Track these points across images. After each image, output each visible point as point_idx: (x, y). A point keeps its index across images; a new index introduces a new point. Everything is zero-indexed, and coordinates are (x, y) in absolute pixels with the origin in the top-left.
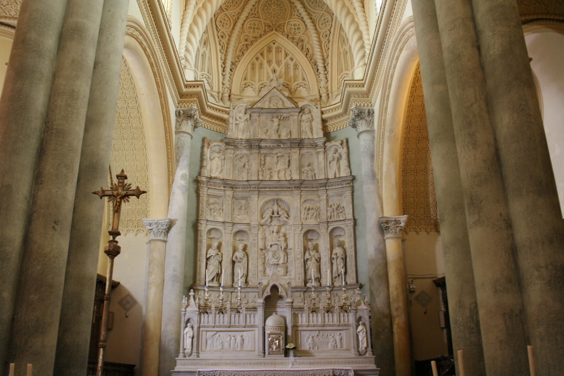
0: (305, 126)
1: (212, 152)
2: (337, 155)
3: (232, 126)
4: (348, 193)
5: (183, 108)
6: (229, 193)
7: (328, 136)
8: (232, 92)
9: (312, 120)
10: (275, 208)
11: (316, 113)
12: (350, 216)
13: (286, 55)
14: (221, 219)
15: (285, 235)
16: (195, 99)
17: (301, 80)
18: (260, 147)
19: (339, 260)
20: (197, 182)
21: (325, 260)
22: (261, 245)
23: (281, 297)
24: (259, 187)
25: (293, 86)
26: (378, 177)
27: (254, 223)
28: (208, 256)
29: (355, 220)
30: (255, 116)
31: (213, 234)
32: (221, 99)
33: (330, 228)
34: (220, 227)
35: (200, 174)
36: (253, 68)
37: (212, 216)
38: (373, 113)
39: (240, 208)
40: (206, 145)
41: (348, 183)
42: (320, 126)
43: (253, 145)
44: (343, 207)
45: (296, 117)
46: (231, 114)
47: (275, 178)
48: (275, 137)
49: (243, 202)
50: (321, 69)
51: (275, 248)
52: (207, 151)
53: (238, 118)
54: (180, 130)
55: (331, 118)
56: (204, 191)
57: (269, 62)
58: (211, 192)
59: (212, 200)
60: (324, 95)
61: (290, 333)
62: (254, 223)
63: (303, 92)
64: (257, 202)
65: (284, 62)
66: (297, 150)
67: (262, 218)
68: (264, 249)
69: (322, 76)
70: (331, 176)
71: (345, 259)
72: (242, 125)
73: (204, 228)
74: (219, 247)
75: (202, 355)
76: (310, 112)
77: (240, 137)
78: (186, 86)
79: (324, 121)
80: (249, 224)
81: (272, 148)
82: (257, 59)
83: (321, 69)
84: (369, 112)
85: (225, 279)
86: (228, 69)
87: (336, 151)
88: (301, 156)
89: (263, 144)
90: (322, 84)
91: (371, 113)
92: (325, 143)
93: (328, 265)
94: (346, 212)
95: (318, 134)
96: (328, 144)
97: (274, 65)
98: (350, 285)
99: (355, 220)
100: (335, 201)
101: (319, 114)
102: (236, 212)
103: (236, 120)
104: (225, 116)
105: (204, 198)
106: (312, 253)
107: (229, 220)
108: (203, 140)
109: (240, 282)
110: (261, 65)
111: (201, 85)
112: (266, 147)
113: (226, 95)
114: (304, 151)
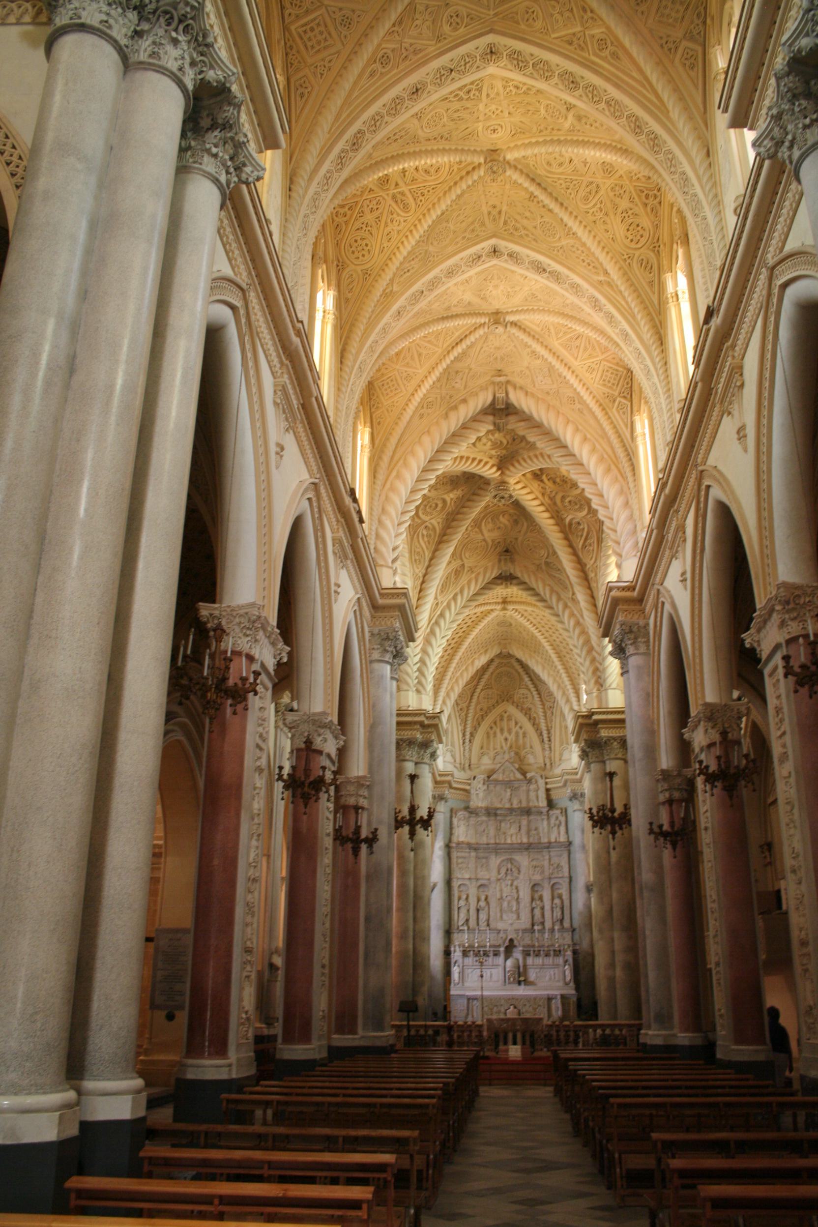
0: (532, 794)
1: (459, 820)
2: (557, 822)
3: (473, 797)
4: (565, 855)
6: (473, 854)
7: (551, 804)
8: (472, 762)
9: (537, 790)
10: (509, 866)
11: (541, 782)
12: (567, 874)
13: (516, 723)
14: (467, 876)
15: (517, 888)
17: (528, 749)
18: (496, 815)
20: (448, 847)
21: (547, 907)
22: (498, 896)
23: (515, 946)
24: (496, 849)
25: (523, 753)
27: (493, 879)
29: (570, 878)
30: (492, 787)
31: (462, 888)
34: (467, 882)
35: (450, 841)
36: (488, 737)
37: (461, 875)
39: (482, 866)
43: (491, 812)
45: (525, 788)
46: (472, 785)
47: (509, 841)
48: (508, 806)
49: (484, 861)
50: (546, 739)
51: (509, 898)
52: (455, 821)
55: (554, 788)
56: (454, 854)
57: (502, 730)
58: (459, 854)
59: (460, 861)
60: (548, 764)
61: (521, 969)
62: (493, 879)
63: (531, 759)
64: (495, 861)
65: (514, 730)
66: (526, 817)
67: (499, 873)
68: (501, 898)
69: (547, 746)
70: (553, 840)
71: (562, 908)
72: (481, 795)
73: (455, 884)
74: (467, 899)
75: (466, 984)
76: (536, 782)
77: (480, 805)
78: (440, 775)
79: (548, 790)
80: (489, 879)
81: (506, 816)
82: (491, 728)
83: (546, 739)
85: (472, 923)
86: (467, 741)
87: (557, 818)
88: (529, 822)
89: (499, 812)
90: (547, 753)
93: (550, 912)
95: (543, 803)
96: (551, 812)
97: (506, 734)
99: (570, 878)
100: (555, 860)
101: (543, 785)
102: (479, 870)
104: (468, 787)
105: (454, 860)
106: (538, 902)
107: (473, 877)
108: (451, 810)
109: (483, 924)
110: (495, 733)
112: (501, 815)
113: (467, 765)
114: (532, 817)
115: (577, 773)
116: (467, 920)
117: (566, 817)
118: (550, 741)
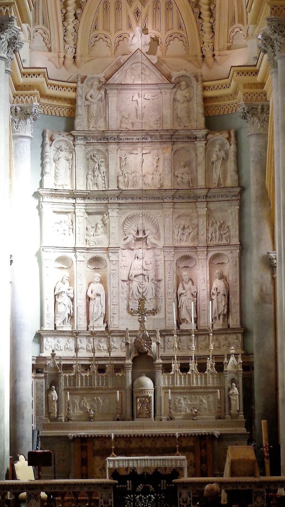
2: (222, 154)
5: (20, 104)
16: (36, 91)
19: (221, 297)
26: (270, 196)
28: (57, 291)
32: (64, 63)
33: (211, 254)
38: (268, 109)
40: (47, 140)
41: (235, 196)
42: (201, 110)
44: (228, 227)
50: (205, 14)
53: (88, 97)
54: (18, 134)
69: (206, 26)
79: (205, 99)
83: (205, 14)
84: (262, 109)
87: (222, 146)
91: (265, 109)
92: (207, 135)
94: (231, 233)
98: (233, 329)
103: (87, 99)
111: (44, 73)
113: (70, 56)
115: (257, 73)
116: (71, 316)
117: (237, 144)
118: (211, 16)
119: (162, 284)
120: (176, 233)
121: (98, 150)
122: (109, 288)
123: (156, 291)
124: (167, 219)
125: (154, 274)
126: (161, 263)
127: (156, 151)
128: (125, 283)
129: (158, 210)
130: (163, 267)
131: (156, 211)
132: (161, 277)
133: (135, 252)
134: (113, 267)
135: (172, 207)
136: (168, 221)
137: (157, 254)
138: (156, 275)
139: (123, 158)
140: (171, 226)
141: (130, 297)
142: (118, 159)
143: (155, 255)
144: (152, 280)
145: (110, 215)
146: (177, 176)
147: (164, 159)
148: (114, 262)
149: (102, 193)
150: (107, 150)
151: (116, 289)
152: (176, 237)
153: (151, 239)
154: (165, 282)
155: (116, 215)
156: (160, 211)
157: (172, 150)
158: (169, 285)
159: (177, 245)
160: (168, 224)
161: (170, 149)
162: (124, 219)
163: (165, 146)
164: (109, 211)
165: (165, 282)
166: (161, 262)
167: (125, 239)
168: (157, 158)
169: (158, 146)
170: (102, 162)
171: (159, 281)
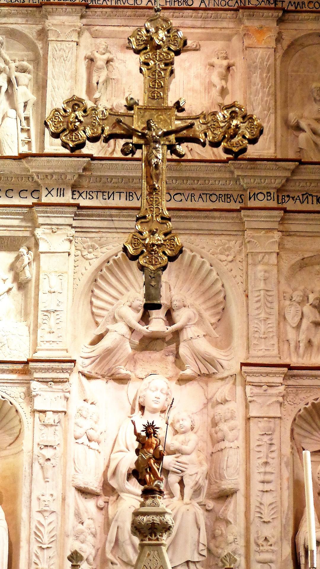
119: (235, 509)
120: (292, 318)
121: (12, 34)
122: (24, 514)
123: (213, 536)
124: (260, 267)
125: (205, 467)
126: (233, 430)
127: (219, 45)
128: (90, 505)
129: (224, 239)
130: (240, 443)
131: (217, 240)
132: (233, 479)
133: (132, 388)
134: (48, 436)
135: (276, 226)
136: (260, 275)
137: (219, 397)
138: (214, 474)
139: (100, 60)
140: (274, 293)
141: (109, 556)
142: (83, 66)
143: (211, 403)
144: (197, 491)
145: (43, 247)
146: (298, 128)
147: (249, 67)
148: (50, 418)
149: (13, 167)
150: (43, 34)
151: (53, 518)
152: (291, 334)
153: (197, 340)
154: (247, 497)
155: (66, 246)
156: (234, 244)
157: (279, 40)
158: (266, 510)
159: (294, 361)
160: (262, 285)
161: (273, 34)
162: (96, 263)
163: (253, 24)
164: (39, 232)
165: (247, 497)
166: (232, 423)
167: (94, 343)
168: (225, 63)
169: (227, 23)
170: (24, 70)
171: (224, 496)
